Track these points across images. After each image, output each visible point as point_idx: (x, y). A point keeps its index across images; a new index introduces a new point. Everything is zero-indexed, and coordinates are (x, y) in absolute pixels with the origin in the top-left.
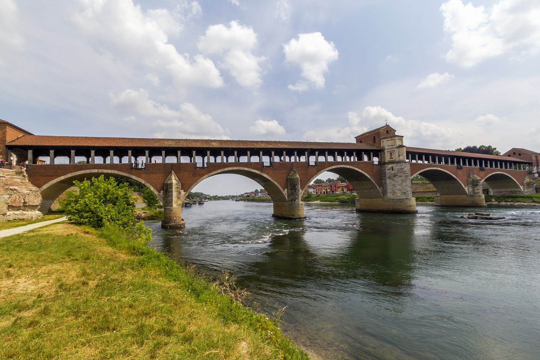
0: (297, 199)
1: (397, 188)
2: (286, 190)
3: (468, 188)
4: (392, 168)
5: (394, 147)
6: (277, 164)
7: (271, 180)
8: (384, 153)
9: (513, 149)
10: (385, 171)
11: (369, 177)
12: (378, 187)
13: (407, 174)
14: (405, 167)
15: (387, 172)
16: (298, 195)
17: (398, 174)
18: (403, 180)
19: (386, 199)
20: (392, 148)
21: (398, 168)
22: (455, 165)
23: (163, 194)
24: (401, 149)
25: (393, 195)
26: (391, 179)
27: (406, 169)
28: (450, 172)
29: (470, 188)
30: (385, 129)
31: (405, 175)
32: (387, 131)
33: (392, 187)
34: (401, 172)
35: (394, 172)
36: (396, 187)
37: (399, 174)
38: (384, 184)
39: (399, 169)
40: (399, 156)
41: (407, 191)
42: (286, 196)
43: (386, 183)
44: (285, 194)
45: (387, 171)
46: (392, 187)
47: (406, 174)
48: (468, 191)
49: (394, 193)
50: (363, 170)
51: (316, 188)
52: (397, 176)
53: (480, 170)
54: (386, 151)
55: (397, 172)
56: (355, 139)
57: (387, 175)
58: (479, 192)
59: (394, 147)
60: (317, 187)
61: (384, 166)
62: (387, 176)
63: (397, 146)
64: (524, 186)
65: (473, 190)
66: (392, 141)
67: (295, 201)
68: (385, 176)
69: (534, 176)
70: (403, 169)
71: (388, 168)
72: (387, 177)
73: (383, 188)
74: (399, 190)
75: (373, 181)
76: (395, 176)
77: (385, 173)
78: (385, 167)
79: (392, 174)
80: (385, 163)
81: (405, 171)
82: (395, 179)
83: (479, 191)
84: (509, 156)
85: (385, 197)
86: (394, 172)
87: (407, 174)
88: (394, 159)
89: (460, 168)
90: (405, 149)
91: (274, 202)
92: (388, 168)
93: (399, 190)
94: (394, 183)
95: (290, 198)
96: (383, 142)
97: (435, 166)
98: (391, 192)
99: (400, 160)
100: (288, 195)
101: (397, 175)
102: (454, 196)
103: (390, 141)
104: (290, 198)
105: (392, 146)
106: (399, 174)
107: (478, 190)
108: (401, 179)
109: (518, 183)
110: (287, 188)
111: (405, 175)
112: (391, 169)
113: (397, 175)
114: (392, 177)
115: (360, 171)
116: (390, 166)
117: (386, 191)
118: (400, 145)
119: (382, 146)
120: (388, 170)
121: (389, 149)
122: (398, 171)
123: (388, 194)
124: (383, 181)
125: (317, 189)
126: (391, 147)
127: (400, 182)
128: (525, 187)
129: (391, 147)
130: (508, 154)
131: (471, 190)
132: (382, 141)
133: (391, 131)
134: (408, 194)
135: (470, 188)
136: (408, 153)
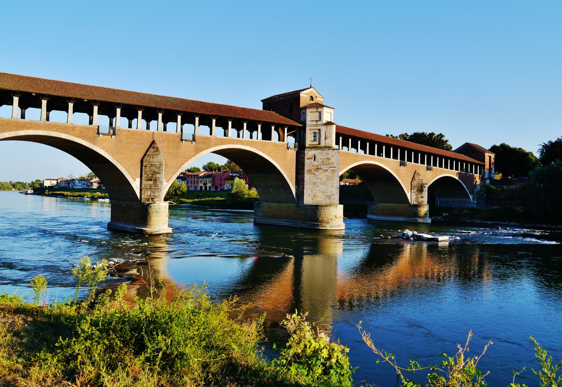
0: (156, 197)
1: (320, 189)
2: (138, 180)
3: (411, 194)
4: (315, 156)
6: (125, 133)
9: (466, 143)
10: (304, 160)
13: (335, 167)
14: (333, 156)
15: (307, 162)
16: (159, 190)
17: (322, 167)
18: (328, 177)
21: (324, 157)
22: (397, 159)
24: (329, 127)
26: (312, 174)
28: (391, 169)
30: (308, 93)
32: (312, 97)
35: (315, 163)
36: (317, 186)
37: (324, 167)
38: (300, 181)
40: (325, 139)
41: (333, 195)
43: (303, 180)
44: (137, 187)
45: (306, 160)
46: (311, 186)
48: (411, 198)
50: (270, 156)
51: (187, 180)
52: (320, 170)
53: (427, 170)
54: (308, 129)
56: (262, 103)
57: (306, 166)
59: (319, 123)
60: (190, 177)
63: (324, 122)
64: (473, 195)
65: (417, 198)
68: (304, 169)
69: (485, 183)
72: (305, 171)
76: (317, 169)
79: (313, 166)
86: (315, 163)
87: (335, 167)
89: (402, 164)
90: (334, 127)
91: (114, 201)
97: (373, 159)
99: (327, 145)
100: (141, 190)
101: (321, 169)
102: (393, 204)
103: (314, 113)
106: (324, 167)
107: (422, 197)
109: (467, 191)
113: (321, 169)
114: (313, 171)
118: (329, 122)
119: (302, 119)
120: (308, 159)
121: (311, 125)
124: (299, 176)
125: (190, 182)
126: (315, 123)
127: (324, 179)
128: (475, 196)
129: (315, 123)
130: (460, 150)
131: (414, 197)
132: (302, 111)
133: (316, 97)
136: (338, 135)
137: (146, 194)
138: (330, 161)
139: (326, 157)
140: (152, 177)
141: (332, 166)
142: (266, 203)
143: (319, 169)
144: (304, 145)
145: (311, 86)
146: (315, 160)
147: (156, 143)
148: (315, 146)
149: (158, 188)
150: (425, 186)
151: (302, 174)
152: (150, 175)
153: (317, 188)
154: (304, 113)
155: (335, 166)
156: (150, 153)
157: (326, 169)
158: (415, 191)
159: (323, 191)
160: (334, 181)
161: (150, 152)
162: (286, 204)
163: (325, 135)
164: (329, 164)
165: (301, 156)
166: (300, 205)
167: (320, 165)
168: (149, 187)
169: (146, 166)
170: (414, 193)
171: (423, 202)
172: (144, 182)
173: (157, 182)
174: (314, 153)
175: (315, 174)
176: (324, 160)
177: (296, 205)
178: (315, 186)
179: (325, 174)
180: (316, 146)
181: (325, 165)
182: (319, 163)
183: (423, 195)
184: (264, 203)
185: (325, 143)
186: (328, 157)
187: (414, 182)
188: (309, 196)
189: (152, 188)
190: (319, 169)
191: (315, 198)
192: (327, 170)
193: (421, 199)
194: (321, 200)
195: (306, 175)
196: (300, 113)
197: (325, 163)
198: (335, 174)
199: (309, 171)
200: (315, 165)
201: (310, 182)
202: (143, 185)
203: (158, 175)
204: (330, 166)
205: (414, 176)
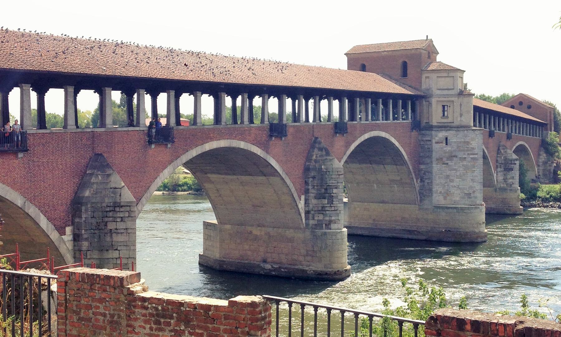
1: (455, 184)
2: (303, 197)
4: (446, 139)
5: (450, 92)
7: (281, 173)
8: (430, 104)
11: (406, 157)
12: (415, 180)
13: (477, 154)
14: (473, 139)
15: (436, 147)
17: (457, 154)
18: (466, 168)
19: (430, 207)
23: (71, 238)
25: (445, 198)
26: (444, 164)
27: (474, 144)
29: (499, 174)
31: (471, 156)
32: (429, 53)
33: (443, 181)
34: (464, 151)
35: (448, 148)
36: (452, 181)
37: (461, 155)
38: (424, 174)
39: (460, 142)
40: (461, 115)
41: (474, 192)
42: (303, 215)
46: (443, 181)
49: (447, 194)
52: (455, 159)
54: (434, 101)
55: (455, 147)
56: (345, 59)
57: (434, 154)
58: (513, 184)
61: (428, 132)
62: (435, 155)
64: (539, 166)
65: (505, 180)
66: (448, 79)
67: (328, 225)
68: (430, 157)
70: (468, 143)
71: (437, 138)
72: (434, 159)
73: (422, 181)
74: (458, 187)
75: (411, 167)
76: (452, 157)
77: (430, 150)
78: (431, 135)
79: (445, 153)
80: (430, 128)
81: (473, 149)
83: (513, 181)
84: (512, 107)
85: (426, 202)
86: (448, 148)
87: (477, 154)
88: (450, 120)
92: (437, 138)
93: (458, 187)
94: (448, 173)
95: (313, 219)
98: (440, 192)
99: (463, 124)
100: (307, 213)
101: (456, 157)
103: (443, 79)
104: (313, 219)
106: (461, 155)
107: (513, 178)
108: (463, 165)
110: (307, 192)
111: (471, 156)
112: (444, 142)
113: (456, 157)
114: (444, 159)
115: (397, 144)
116: (442, 135)
117: (431, 190)
119: (424, 87)
120: (437, 143)
121: (440, 96)
122: (458, 147)
123: (434, 195)
124: (422, 167)
129: (446, 92)
131: (501, 178)
132: (424, 76)
134: (476, 197)
135: (499, 174)
137: (316, 218)
138: (471, 146)
139: (463, 140)
140: (325, 193)
141: (471, 152)
142: (359, 203)
143: (454, 156)
144: (429, 123)
145: (427, 36)
146: (447, 144)
147: (320, 143)
148: (446, 124)
149: (336, 209)
150: (516, 162)
151: (428, 164)
152: (323, 191)
153: (452, 184)
155: (476, 152)
156: (319, 158)
157: (464, 156)
158: (502, 169)
159: (460, 187)
160: (475, 174)
161: (316, 157)
162: (399, 205)
163: (461, 110)
164: (468, 151)
165: (424, 139)
166: (425, 207)
167: (455, 151)
168: (320, 208)
169: (314, 178)
170: (502, 173)
171: (513, 184)
172: (313, 202)
173: (334, 200)
174: (447, 134)
175: (447, 164)
176: (460, 145)
177: (417, 206)
179: (461, 163)
180: (449, 124)
181: (461, 151)
182: (453, 149)
183: (514, 175)
184: (355, 203)
186: (466, 140)
187: (501, 157)
188: (439, 195)
189: (327, 209)
190: (454, 156)
191: (448, 198)
192: (465, 158)
193: (511, 181)
194: (458, 199)
195: (433, 165)
196: (420, 78)
197: (462, 149)
198: (477, 164)
199: (440, 160)
200: (448, 151)
201: (441, 174)
202: (311, 206)
203: (335, 191)
204: (469, 152)
205: (499, 149)
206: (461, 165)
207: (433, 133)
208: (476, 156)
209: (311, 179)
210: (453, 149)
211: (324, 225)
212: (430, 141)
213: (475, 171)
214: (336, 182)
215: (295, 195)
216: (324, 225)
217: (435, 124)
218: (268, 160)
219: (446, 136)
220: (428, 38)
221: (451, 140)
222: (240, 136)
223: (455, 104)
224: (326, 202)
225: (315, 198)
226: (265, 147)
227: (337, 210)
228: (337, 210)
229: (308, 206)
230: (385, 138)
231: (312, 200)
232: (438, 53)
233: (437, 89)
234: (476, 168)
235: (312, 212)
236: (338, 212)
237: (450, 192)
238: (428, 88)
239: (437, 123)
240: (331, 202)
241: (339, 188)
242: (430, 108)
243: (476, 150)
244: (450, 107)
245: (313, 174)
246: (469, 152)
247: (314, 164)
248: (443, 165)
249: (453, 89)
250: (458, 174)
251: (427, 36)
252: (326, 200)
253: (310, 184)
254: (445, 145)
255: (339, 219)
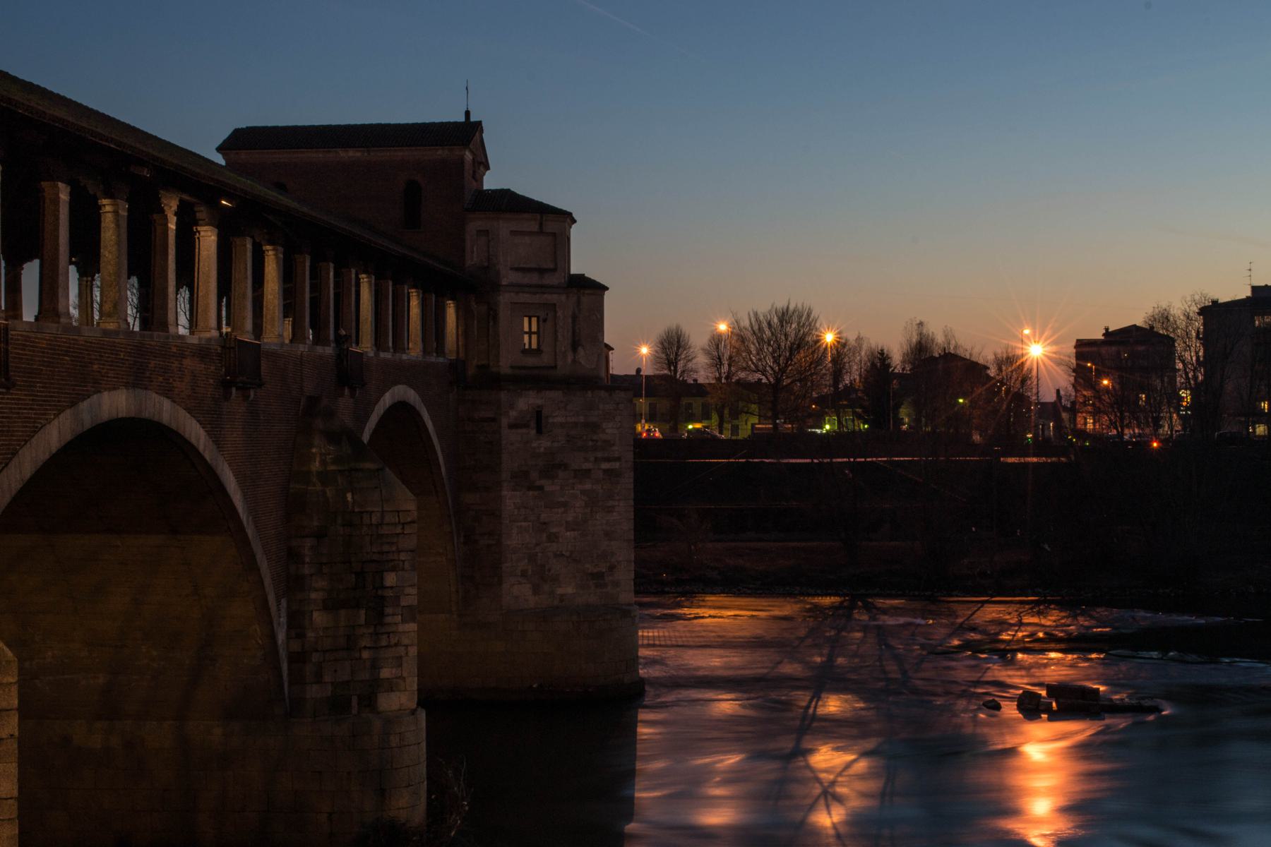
13: (618, 459)
20: (543, 288)
25: (536, 590)
26: (529, 489)
31: (605, 466)
35: (544, 444)
36: (553, 538)
40: (575, 346)
41: (612, 568)
47: (608, 460)
54: (504, 299)
59: (550, 280)
67: (369, 702)
71: (513, 414)
76: (552, 468)
82: (549, 486)
86: (544, 444)
87: (618, 459)
88: (546, 359)
96: (480, 232)
98: (524, 574)
100: (297, 659)
105: (542, 271)
111: (605, 466)
112: (533, 424)
116: (526, 402)
120: (512, 426)
121: (518, 288)
126: (534, 279)
129: (534, 279)
137: (327, 678)
139: (582, 419)
145: (467, 114)
146: (539, 431)
149: (393, 641)
154: (486, 232)
156: (333, 468)
157: (586, 466)
161: (323, 463)
173: (389, 610)
174: (539, 402)
175: (541, 488)
178: (545, 535)
182: (556, 445)
185: (574, 361)
192: (590, 470)
194: (570, 590)
195: (505, 493)
200: (542, 450)
204: (599, 455)
206: (579, 492)
207: (503, 396)
208: (616, 465)
209: (309, 542)
210: (556, 445)
211: (355, 701)
212: (493, 420)
213: (613, 507)
214: (394, 549)
215: (271, 598)
216: (355, 701)
217: (508, 371)
218: (219, 472)
219: (539, 407)
220: (473, 119)
221: (551, 420)
222: (161, 379)
223: (559, 313)
224: (362, 620)
225: (327, 606)
226: (214, 425)
227: (396, 645)
228: (396, 645)
229: (301, 636)
230: (413, 408)
231: (315, 615)
232: (487, 168)
233: (511, 269)
234: (617, 498)
235: (316, 657)
236: (401, 650)
237: (549, 570)
238: (486, 264)
239: (512, 367)
240: (377, 618)
241: (403, 569)
242: (491, 324)
243: (615, 448)
244: (545, 321)
245: (316, 523)
246: (599, 455)
247: (319, 488)
248: (531, 493)
249: (554, 270)
250: (570, 519)
251: (467, 114)
252: (362, 612)
253: (307, 560)
254: (533, 432)
255: (405, 674)
